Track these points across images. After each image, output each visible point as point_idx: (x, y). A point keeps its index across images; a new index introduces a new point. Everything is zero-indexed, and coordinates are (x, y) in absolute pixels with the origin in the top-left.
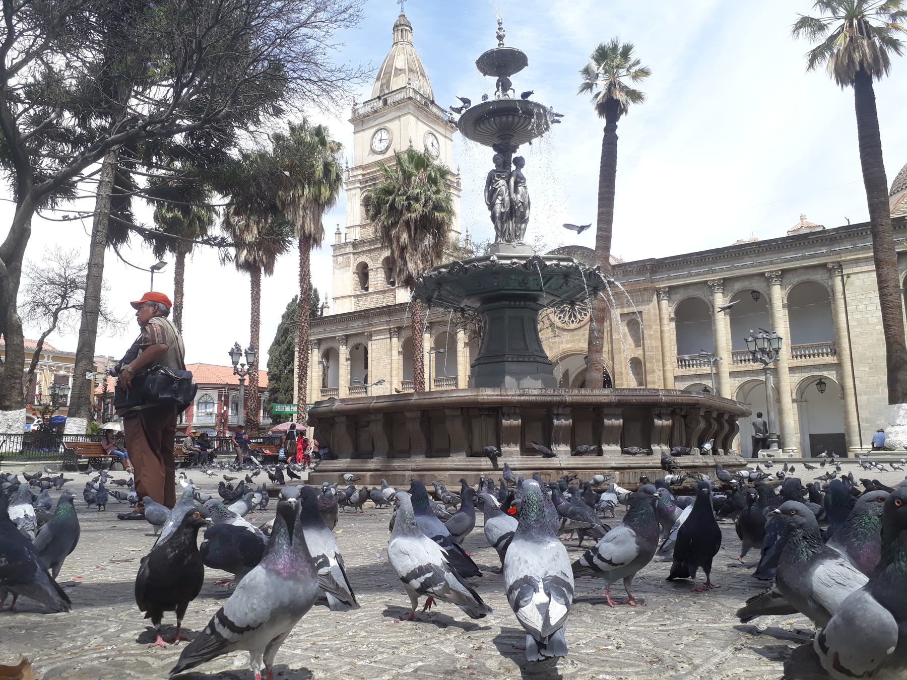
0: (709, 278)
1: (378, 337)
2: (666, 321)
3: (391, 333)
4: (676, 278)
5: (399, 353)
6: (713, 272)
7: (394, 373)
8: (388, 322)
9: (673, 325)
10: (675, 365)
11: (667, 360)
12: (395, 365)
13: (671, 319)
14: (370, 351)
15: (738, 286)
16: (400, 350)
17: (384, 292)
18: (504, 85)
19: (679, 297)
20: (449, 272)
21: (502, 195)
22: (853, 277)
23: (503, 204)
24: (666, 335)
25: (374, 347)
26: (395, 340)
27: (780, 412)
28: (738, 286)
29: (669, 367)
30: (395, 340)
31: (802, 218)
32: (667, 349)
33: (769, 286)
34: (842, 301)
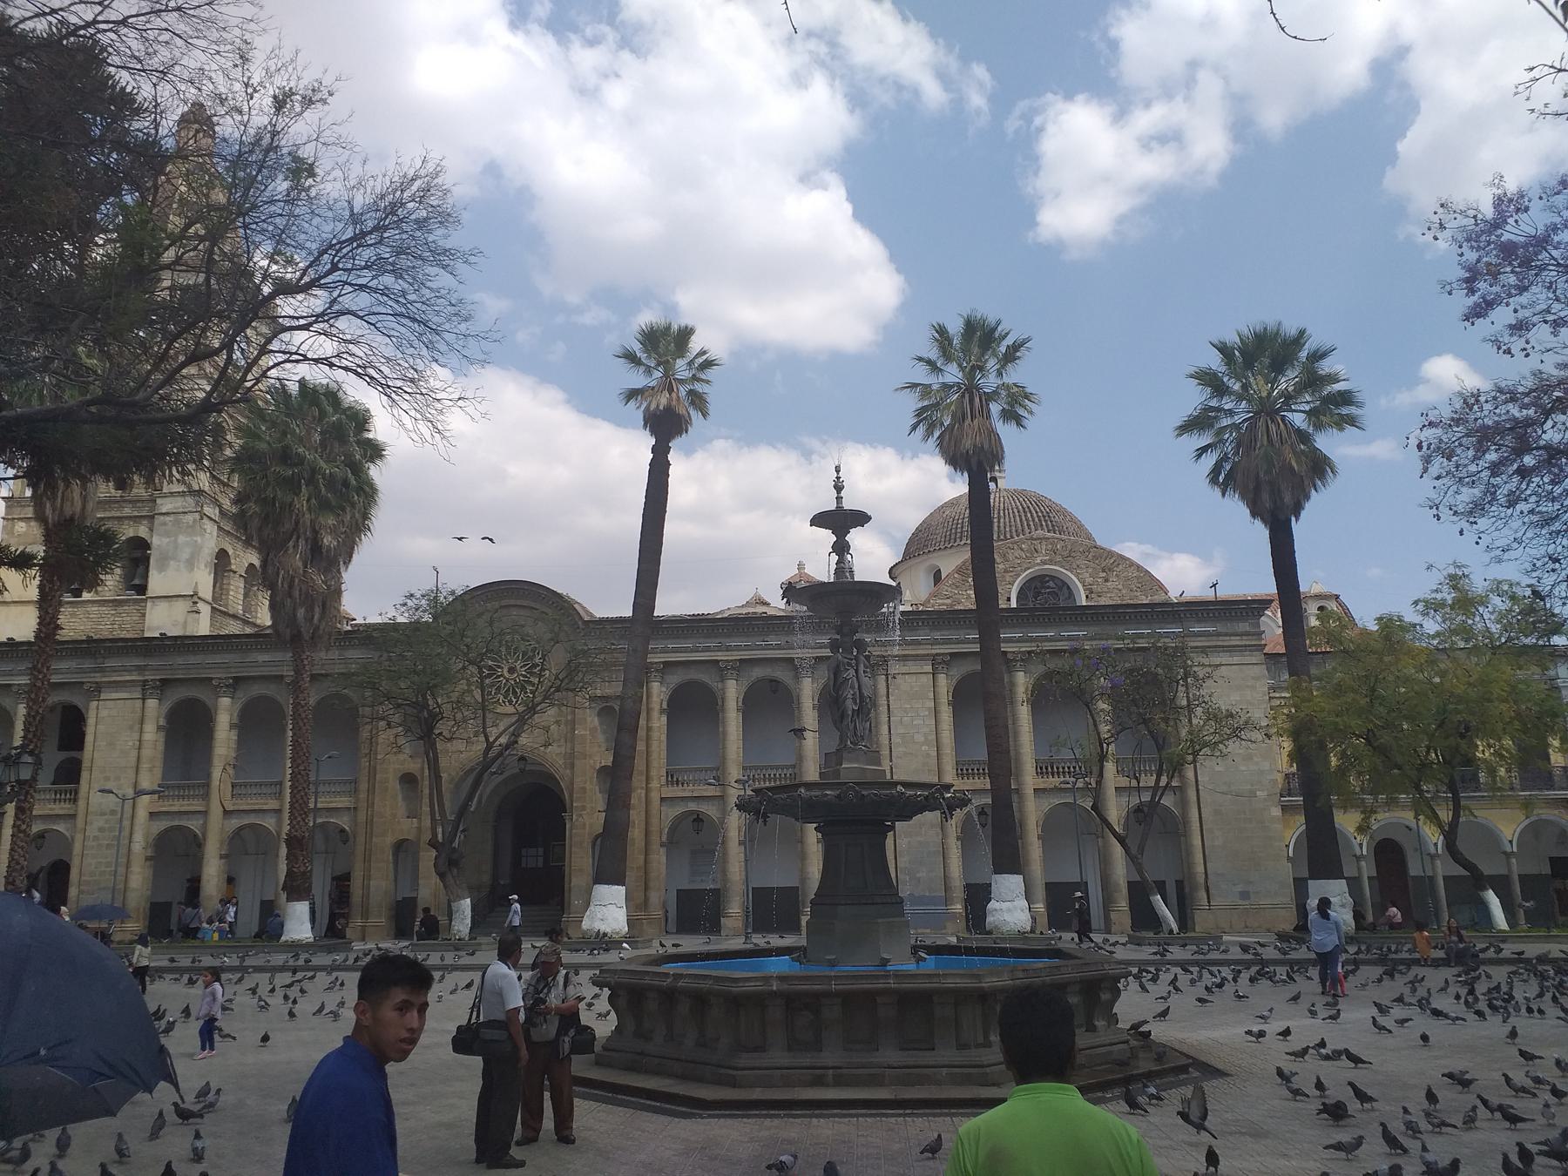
0: (720, 656)
1: (115, 696)
2: (655, 714)
3: (146, 689)
4: (675, 651)
5: (159, 728)
6: (728, 649)
7: (145, 766)
8: (141, 669)
9: (664, 719)
10: (663, 779)
11: (653, 773)
12: (147, 752)
13: (662, 711)
14: (91, 721)
15: (758, 673)
16: (162, 722)
17: (116, 603)
18: (841, 548)
19: (675, 679)
20: (838, 797)
21: (852, 687)
22: (900, 679)
23: (854, 700)
24: (655, 735)
25: (104, 713)
26: (152, 703)
27: (803, 857)
28: (758, 673)
29: (654, 784)
30: (152, 703)
31: (801, 566)
32: (654, 755)
33: (797, 677)
34: (883, 709)
